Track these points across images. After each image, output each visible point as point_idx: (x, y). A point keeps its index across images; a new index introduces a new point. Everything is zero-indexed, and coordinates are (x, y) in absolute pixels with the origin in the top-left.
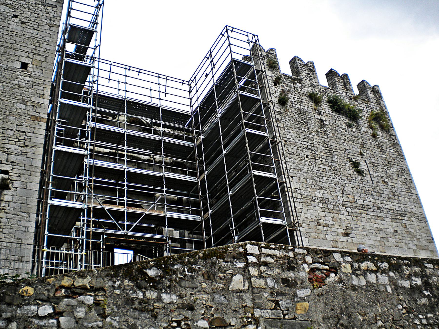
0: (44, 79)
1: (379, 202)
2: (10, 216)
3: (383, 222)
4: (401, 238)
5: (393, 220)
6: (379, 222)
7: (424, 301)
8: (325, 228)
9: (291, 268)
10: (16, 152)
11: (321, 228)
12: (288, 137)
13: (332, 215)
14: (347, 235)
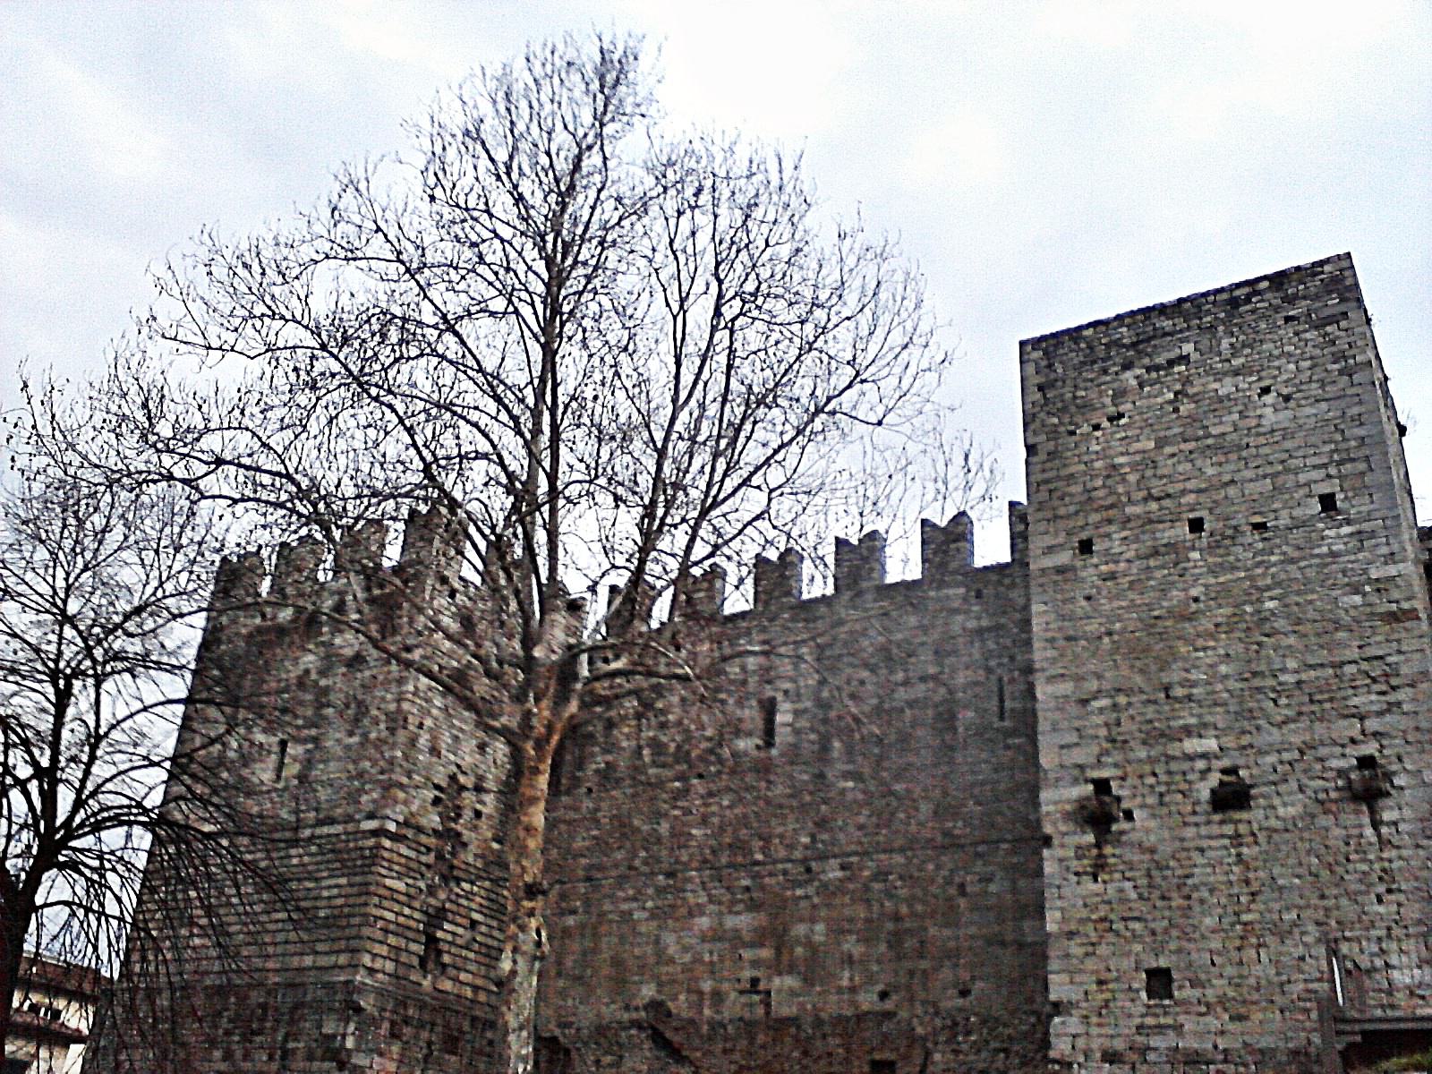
0: (1378, 515)
2: (1405, 853)
10: (1375, 708)
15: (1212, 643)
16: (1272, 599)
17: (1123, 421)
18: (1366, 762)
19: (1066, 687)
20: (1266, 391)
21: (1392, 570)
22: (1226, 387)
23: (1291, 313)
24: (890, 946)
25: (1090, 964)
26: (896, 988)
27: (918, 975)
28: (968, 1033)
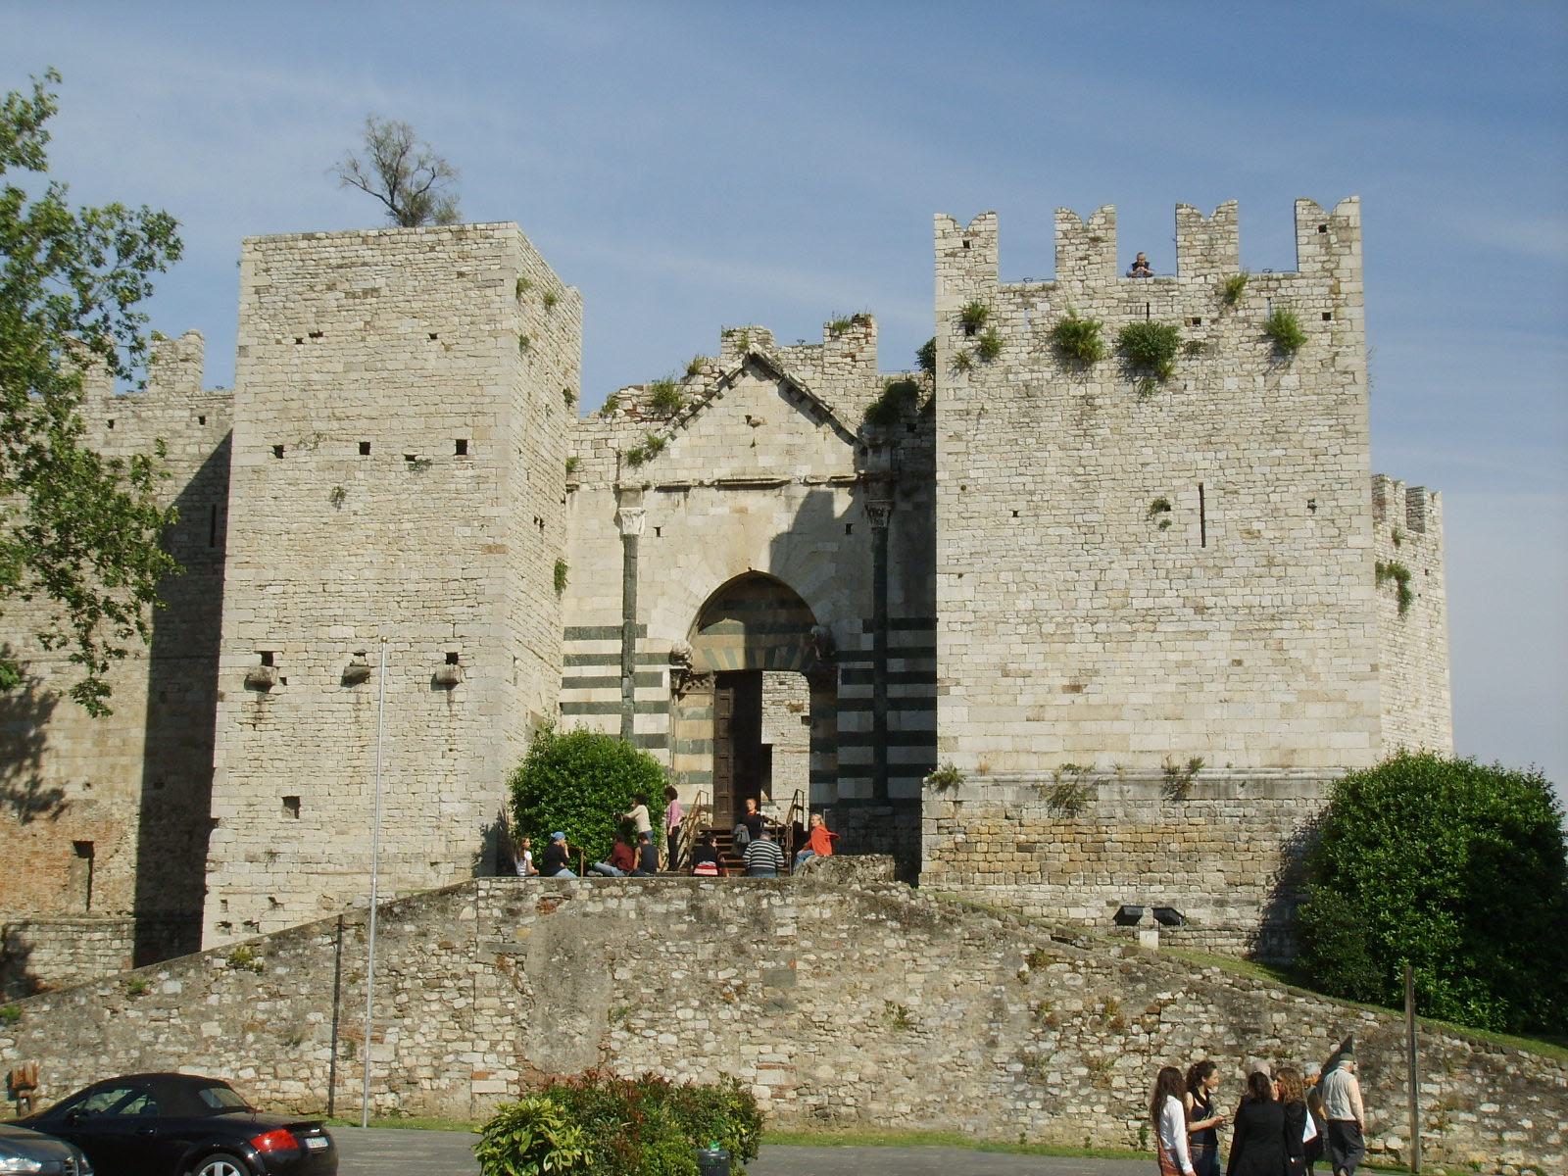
1: (1208, 592)
3: (1199, 645)
4: (1249, 677)
5: (1237, 635)
6: (1188, 645)
7: (684, 927)
8: (1020, 681)
9: (519, 899)
10: (464, 617)
11: (1009, 680)
12: (973, 474)
13: (1046, 648)
14: (1076, 688)
15: (362, 551)
16: (409, 521)
17: (320, 340)
18: (452, 658)
19: (248, 573)
20: (433, 337)
21: (495, 511)
22: (406, 326)
23: (463, 269)
24: (95, 744)
25: (245, 791)
26: (98, 781)
27: (118, 770)
28: (160, 819)
